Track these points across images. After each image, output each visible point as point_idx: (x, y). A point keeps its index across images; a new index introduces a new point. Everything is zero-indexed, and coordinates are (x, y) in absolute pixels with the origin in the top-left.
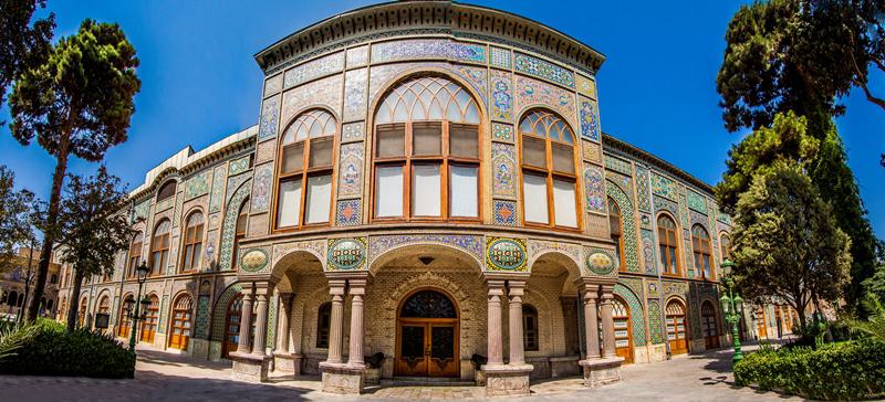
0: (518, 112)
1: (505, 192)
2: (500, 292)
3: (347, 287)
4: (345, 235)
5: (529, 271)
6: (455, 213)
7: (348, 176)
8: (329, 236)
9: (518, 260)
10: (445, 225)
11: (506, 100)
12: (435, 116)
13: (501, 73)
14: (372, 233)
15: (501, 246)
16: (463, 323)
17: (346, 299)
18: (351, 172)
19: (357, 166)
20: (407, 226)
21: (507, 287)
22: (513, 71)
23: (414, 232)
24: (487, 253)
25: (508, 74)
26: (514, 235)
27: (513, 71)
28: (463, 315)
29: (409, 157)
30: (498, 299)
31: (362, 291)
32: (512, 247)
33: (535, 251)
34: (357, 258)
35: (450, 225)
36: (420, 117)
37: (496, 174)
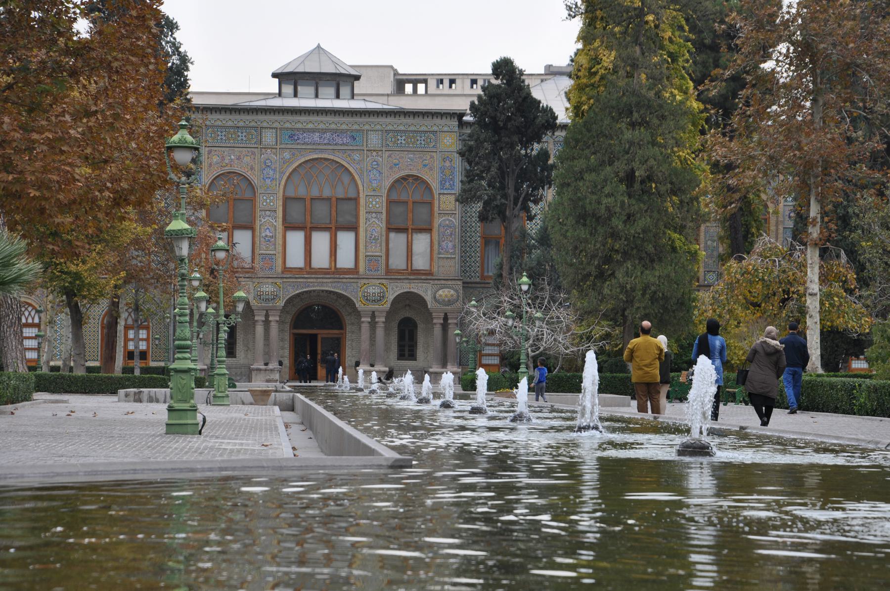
0: (387, 184)
1: (377, 250)
2: (369, 320)
3: (267, 316)
4: (266, 280)
5: (389, 306)
6: (338, 266)
7: (266, 236)
8: (254, 280)
9: (381, 298)
10: (332, 276)
11: (377, 175)
12: (327, 193)
13: (374, 154)
14: (285, 280)
15: (371, 290)
16: (348, 336)
17: (267, 323)
18: (268, 233)
19: (273, 229)
20: (308, 269)
21: (373, 315)
22: (384, 149)
23: (312, 280)
24: (360, 294)
25: (380, 153)
26: (380, 281)
27: (384, 149)
28: (348, 328)
29: (309, 225)
30: (368, 325)
31: (278, 318)
32: (377, 290)
33: (394, 290)
34: (275, 297)
35: (334, 272)
36: (315, 193)
37: (369, 235)
